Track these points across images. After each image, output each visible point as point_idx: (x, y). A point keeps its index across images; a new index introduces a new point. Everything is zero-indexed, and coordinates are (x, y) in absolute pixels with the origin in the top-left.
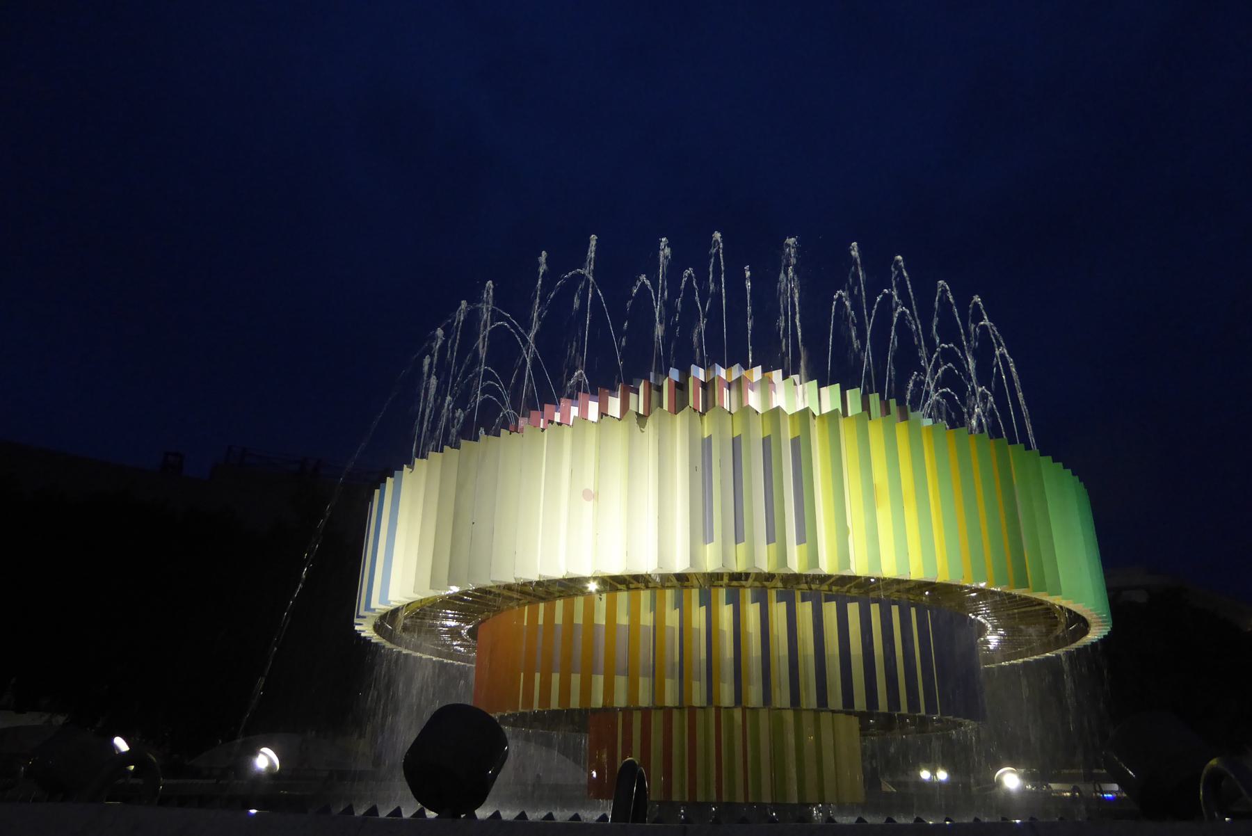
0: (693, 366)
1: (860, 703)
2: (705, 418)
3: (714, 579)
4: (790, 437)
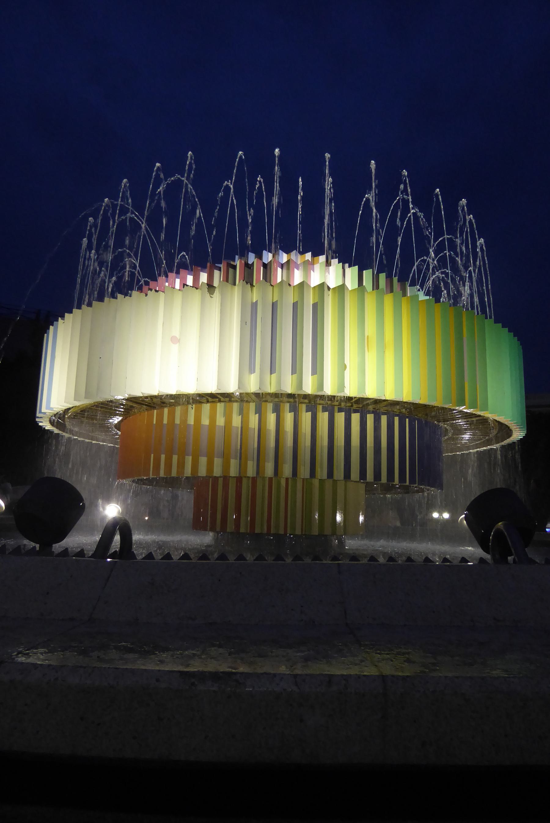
0: (264, 252)
1: (370, 476)
4: (312, 303)
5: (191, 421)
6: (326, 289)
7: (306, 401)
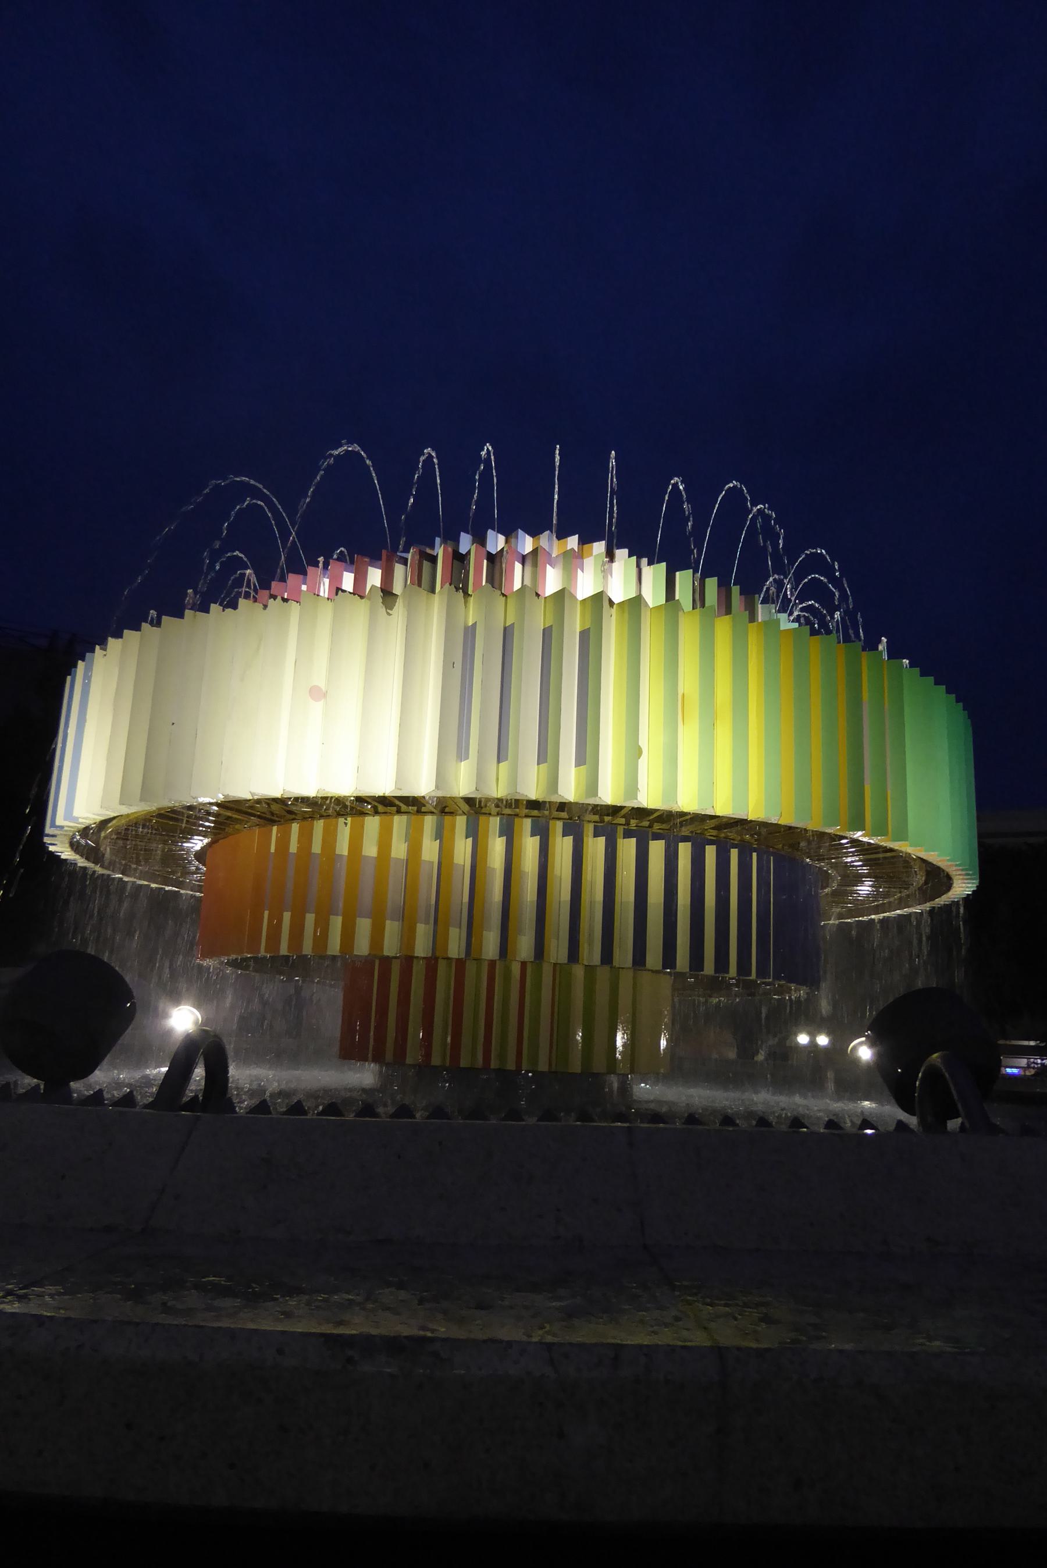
0: (490, 532)
2: (471, 600)
3: (475, 806)
4: (578, 630)
5: (343, 847)
6: (606, 604)
7: (564, 815)
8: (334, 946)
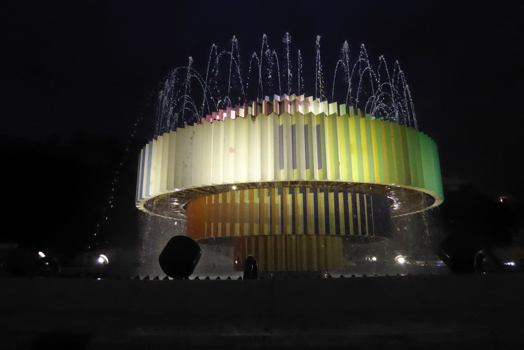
0: (275, 95)
1: (343, 232)
2: (280, 117)
3: (284, 184)
4: (316, 125)
8: (237, 233)
